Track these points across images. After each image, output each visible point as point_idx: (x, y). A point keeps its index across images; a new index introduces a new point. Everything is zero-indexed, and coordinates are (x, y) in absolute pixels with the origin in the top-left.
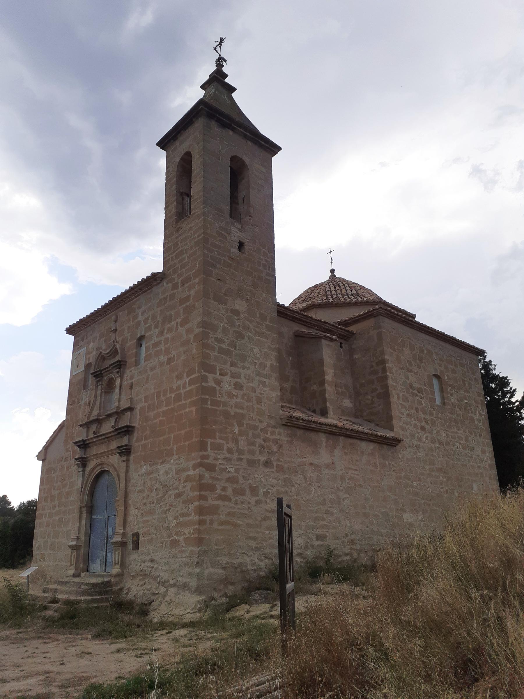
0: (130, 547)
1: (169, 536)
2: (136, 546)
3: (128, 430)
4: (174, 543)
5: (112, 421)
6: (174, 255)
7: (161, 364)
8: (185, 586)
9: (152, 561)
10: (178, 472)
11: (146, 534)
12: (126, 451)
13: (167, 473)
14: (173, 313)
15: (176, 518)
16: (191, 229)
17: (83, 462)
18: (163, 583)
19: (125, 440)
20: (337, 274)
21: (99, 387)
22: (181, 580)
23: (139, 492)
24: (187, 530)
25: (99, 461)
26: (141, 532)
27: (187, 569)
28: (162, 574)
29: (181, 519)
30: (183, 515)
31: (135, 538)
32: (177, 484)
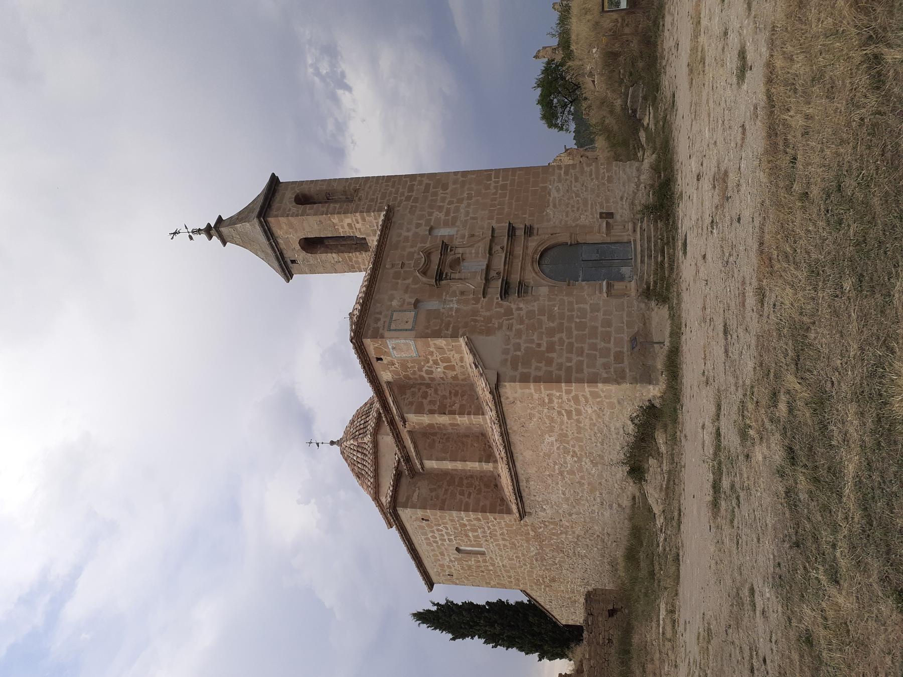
0: (610, 221)
1: (604, 184)
2: (610, 215)
3: (512, 230)
4: (610, 180)
5: (496, 248)
6: (379, 201)
7: (469, 205)
8: (638, 170)
9: (622, 198)
10: (560, 181)
11: (602, 206)
13: (558, 190)
14: (430, 198)
15: (592, 179)
16: (370, 187)
17: (523, 289)
18: (638, 186)
19: (520, 233)
20: (338, 435)
21: (453, 276)
23: (567, 216)
24: (602, 171)
25: (529, 267)
26: (599, 211)
27: (628, 170)
28: (631, 189)
29: (594, 176)
30: (591, 175)
31: (604, 215)
32: (568, 182)
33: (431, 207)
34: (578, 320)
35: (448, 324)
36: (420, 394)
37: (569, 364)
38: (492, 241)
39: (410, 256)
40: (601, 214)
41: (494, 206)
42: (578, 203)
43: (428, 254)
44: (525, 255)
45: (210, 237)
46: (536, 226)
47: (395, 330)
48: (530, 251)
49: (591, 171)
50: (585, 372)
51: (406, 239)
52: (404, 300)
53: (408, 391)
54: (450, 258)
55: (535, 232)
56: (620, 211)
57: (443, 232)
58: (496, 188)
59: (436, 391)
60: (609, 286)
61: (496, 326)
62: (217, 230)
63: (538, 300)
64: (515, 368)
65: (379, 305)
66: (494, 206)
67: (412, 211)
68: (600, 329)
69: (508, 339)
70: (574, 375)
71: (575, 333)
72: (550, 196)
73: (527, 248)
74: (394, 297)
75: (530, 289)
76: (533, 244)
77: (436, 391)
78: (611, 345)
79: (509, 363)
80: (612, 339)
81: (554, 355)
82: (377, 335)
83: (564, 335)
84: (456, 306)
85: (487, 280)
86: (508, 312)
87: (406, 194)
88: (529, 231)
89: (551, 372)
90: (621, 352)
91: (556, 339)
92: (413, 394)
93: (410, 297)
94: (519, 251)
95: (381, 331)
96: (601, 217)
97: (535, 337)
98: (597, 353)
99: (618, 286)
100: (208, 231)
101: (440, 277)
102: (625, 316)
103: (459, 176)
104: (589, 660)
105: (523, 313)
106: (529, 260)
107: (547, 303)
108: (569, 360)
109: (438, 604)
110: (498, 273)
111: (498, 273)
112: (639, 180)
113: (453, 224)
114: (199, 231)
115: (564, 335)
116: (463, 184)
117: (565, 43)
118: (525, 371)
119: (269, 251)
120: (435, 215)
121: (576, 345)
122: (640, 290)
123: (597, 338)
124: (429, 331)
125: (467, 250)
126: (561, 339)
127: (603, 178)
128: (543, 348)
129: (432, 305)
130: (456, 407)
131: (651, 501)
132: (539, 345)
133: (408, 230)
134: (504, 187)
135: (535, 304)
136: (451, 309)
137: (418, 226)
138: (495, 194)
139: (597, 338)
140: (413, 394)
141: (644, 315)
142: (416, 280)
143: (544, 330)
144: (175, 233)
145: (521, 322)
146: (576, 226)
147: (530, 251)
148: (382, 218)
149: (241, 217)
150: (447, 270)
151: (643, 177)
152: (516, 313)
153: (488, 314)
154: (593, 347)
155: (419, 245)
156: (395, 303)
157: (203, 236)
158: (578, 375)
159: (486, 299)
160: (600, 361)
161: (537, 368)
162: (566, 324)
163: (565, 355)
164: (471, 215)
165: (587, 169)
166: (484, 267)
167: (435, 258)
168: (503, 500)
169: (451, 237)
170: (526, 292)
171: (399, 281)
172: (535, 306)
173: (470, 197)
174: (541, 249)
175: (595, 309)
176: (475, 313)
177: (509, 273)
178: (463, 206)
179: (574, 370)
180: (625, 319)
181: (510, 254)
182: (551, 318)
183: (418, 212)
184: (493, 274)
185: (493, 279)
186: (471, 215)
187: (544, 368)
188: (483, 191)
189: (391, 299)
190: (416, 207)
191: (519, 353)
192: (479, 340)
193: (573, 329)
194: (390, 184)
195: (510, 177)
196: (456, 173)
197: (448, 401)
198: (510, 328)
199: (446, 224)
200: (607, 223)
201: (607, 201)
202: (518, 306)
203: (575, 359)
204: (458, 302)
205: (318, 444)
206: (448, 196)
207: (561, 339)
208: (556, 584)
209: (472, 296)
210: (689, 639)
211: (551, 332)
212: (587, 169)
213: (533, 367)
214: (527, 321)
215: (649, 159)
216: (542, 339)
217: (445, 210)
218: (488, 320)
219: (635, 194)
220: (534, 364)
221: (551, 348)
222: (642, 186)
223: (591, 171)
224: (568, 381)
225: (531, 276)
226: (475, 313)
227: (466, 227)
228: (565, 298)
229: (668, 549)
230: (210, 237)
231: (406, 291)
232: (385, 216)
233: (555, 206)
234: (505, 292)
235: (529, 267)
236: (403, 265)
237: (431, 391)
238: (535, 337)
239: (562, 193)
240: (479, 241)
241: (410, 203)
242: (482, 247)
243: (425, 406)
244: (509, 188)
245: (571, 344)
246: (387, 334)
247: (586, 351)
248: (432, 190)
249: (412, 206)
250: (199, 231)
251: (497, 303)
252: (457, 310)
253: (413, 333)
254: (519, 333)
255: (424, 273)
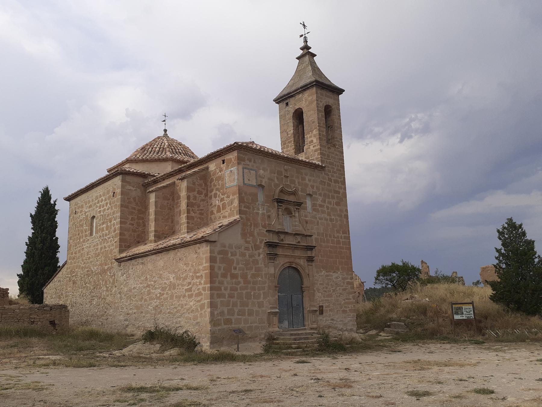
0: (318, 313)
1: (341, 308)
2: (321, 312)
3: (311, 248)
4: (344, 312)
5: (299, 238)
7: (326, 220)
8: (351, 330)
9: (332, 320)
10: (343, 279)
11: (328, 306)
12: (310, 260)
13: (337, 278)
15: (344, 300)
17: (273, 257)
18: (340, 330)
19: (309, 253)
21: (280, 210)
22: (349, 328)
23: (320, 284)
25: (287, 260)
26: (324, 305)
27: (351, 323)
29: (347, 301)
30: (347, 299)
31: (321, 308)
32: (342, 284)
33: (325, 195)
34: (252, 293)
35: (249, 208)
36: (200, 189)
37: (223, 288)
38: (303, 235)
39: (293, 182)
40: (322, 306)
41: (326, 236)
42: (329, 291)
43: (294, 193)
44: (295, 257)
45: (302, 49)
46: (313, 264)
47: (243, 172)
48: (297, 261)
49: (349, 299)
50: (218, 300)
51: (303, 179)
52: (264, 178)
53: (202, 182)
54: (292, 208)
55: (310, 264)
56: (324, 319)
57: (309, 203)
58: (338, 237)
59: (203, 200)
60: (276, 313)
61: (248, 240)
62: (307, 53)
63: (265, 267)
64: (220, 253)
65: (260, 161)
66: (326, 236)
67: (322, 182)
68: (246, 308)
69: (239, 247)
70: (216, 292)
71: (244, 292)
72: (334, 272)
73: (299, 259)
74: (265, 172)
75: (273, 261)
76: (302, 262)
77: (203, 200)
78: (236, 316)
79: (223, 249)
80: (240, 317)
81: (229, 278)
82: (240, 160)
83: (242, 284)
84: (260, 212)
85: (278, 233)
86: (257, 247)
87: (333, 178)
88: (310, 260)
89: (217, 277)
90: (231, 323)
91: (240, 279)
92: (200, 185)
93: (265, 182)
94: (298, 253)
95: (243, 163)
96: (320, 307)
97: (240, 265)
98: (231, 307)
99: (276, 319)
100: (306, 48)
101: (280, 201)
102: (256, 324)
103: (345, 213)
104: (19, 309)
105: (256, 257)
106: (292, 260)
107: (263, 272)
108: (226, 289)
109: (55, 204)
110: (282, 240)
111: (282, 240)
112: (345, 331)
113: (314, 210)
114: (306, 41)
115: (242, 284)
116: (340, 216)
117: (432, 280)
118: (218, 259)
119: (294, 88)
120: (320, 197)
121: (236, 293)
122: (273, 334)
123: (240, 306)
124: (243, 195)
125: (297, 219)
126: (239, 283)
127: (345, 307)
128: (233, 271)
129: (261, 197)
130: (192, 214)
131: (131, 347)
132: (235, 268)
133: (309, 180)
134: (338, 242)
135: (263, 265)
136: (258, 209)
137: (313, 187)
138: (334, 237)
139: (240, 306)
140: (200, 185)
141: (257, 337)
142: (277, 186)
143: (245, 271)
144: (304, 25)
145: (250, 256)
146: (314, 290)
147: (297, 261)
148: (317, 163)
149: (316, 69)
150: (284, 206)
151: (346, 333)
152: (256, 252)
153: (256, 234)
154: (235, 305)
155: (300, 187)
156: (261, 172)
157: (302, 45)
158: (215, 295)
159: (265, 232)
160: (226, 310)
161: (219, 268)
162: (249, 286)
163: (229, 286)
164: (320, 221)
165: (351, 296)
166: (286, 231)
167: (292, 198)
168: (129, 247)
169: (305, 208)
170: (270, 259)
171: (276, 175)
172: (261, 265)
173: (331, 220)
174: (299, 268)
175: (260, 305)
176: (256, 225)
177: (283, 247)
178: (326, 216)
179: (219, 292)
180: (254, 325)
181: (295, 247)
182: (254, 276)
183: (321, 186)
184: (282, 236)
185: (279, 236)
186: (320, 221)
187: (220, 272)
188: (335, 229)
189: (264, 170)
190: (325, 185)
191: (230, 255)
192: (238, 229)
193: (246, 291)
194: (339, 168)
195: (344, 246)
196: (347, 211)
197: (196, 208)
198: (247, 249)
199: (314, 205)
200: (316, 311)
201: (330, 310)
202: (262, 253)
203: (227, 293)
204: (263, 214)
205: (164, 121)
206: (332, 206)
207: (239, 283)
208: (72, 285)
209: (267, 223)
210: (36, 376)
211: (244, 276)
212: (351, 296)
213: (220, 265)
214: (251, 260)
215: (358, 337)
216: (239, 270)
217: (323, 204)
218: (252, 234)
219: (336, 328)
220: (223, 266)
221: (233, 276)
222: (341, 333)
223: (349, 299)
224: (211, 289)
225: (281, 261)
226: (256, 225)
227: (312, 218)
228: (267, 285)
229: (98, 359)
230: (302, 49)
231: (270, 179)
232: (318, 165)
233: (327, 276)
234: (270, 245)
235: (287, 260)
236: (287, 177)
237: (202, 196)
238: (240, 265)
239: (335, 280)
240: (303, 227)
241: (327, 181)
242: (300, 229)
243: (193, 193)
244: (338, 245)
245: (236, 290)
246: (241, 167)
247: (232, 300)
248: (336, 195)
249: (325, 182)
250: (306, 41)
251: (263, 240)
252: (257, 213)
253: (242, 184)
254: (243, 255)
255: (282, 191)
